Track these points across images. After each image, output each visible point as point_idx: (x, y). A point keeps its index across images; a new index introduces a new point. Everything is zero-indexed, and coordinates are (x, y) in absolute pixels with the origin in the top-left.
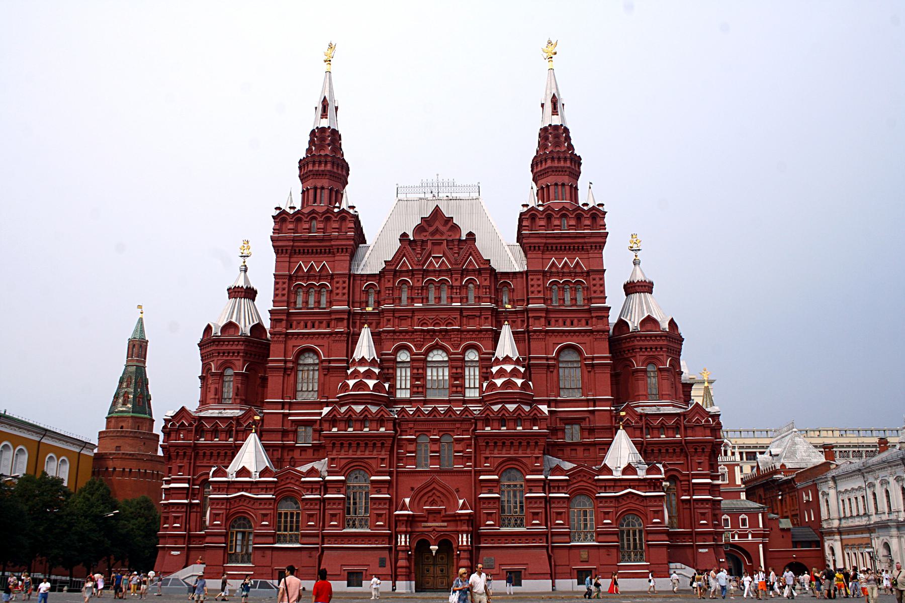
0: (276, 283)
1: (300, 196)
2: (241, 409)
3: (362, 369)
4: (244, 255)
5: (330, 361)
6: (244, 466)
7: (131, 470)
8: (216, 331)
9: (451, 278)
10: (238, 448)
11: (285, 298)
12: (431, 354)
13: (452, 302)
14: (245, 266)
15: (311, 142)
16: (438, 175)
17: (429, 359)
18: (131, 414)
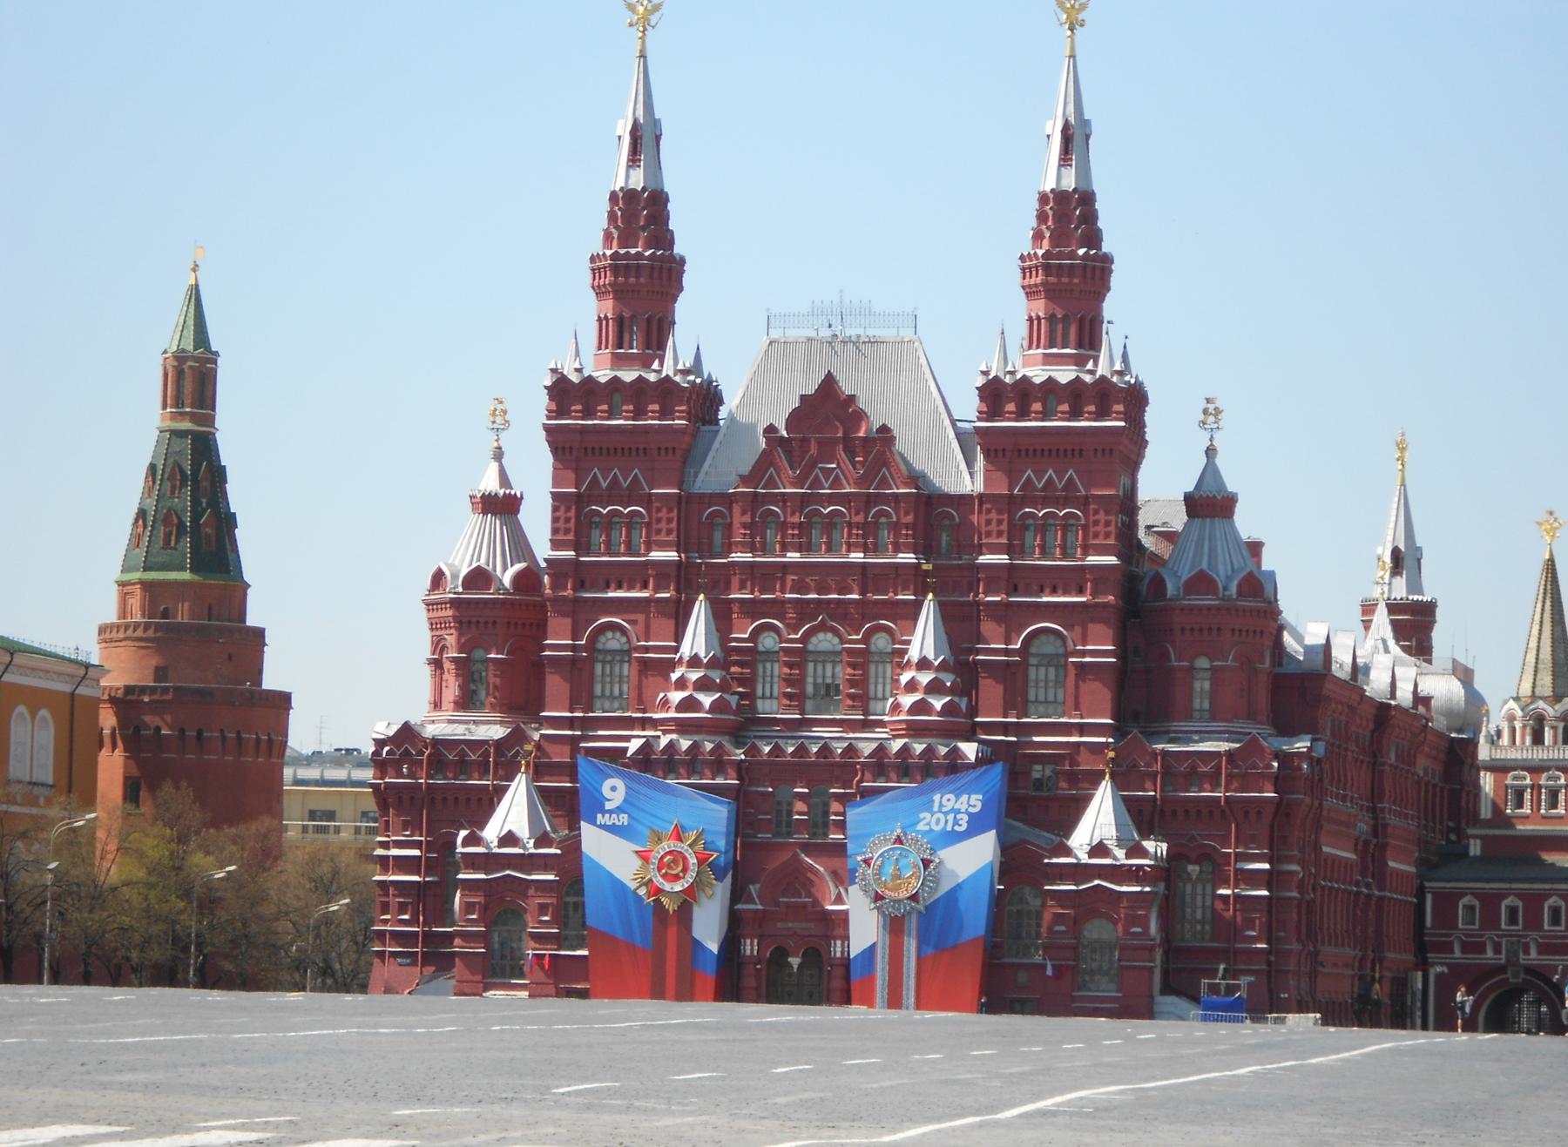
0: (555, 509)
1: (595, 325)
2: (501, 723)
3: (694, 676)
4: (496, 426)
5: (647, 649)
6: (510, 831)
7: (200, 733)
8: (454, 588)
9: (849, 509)
10: (500, 792)
11: (571, 537)
12: (814, 640)
13: (849, 551)
14: (500, 448)
15: (612, 217)
16: (841, 291)
17: (811, 647)
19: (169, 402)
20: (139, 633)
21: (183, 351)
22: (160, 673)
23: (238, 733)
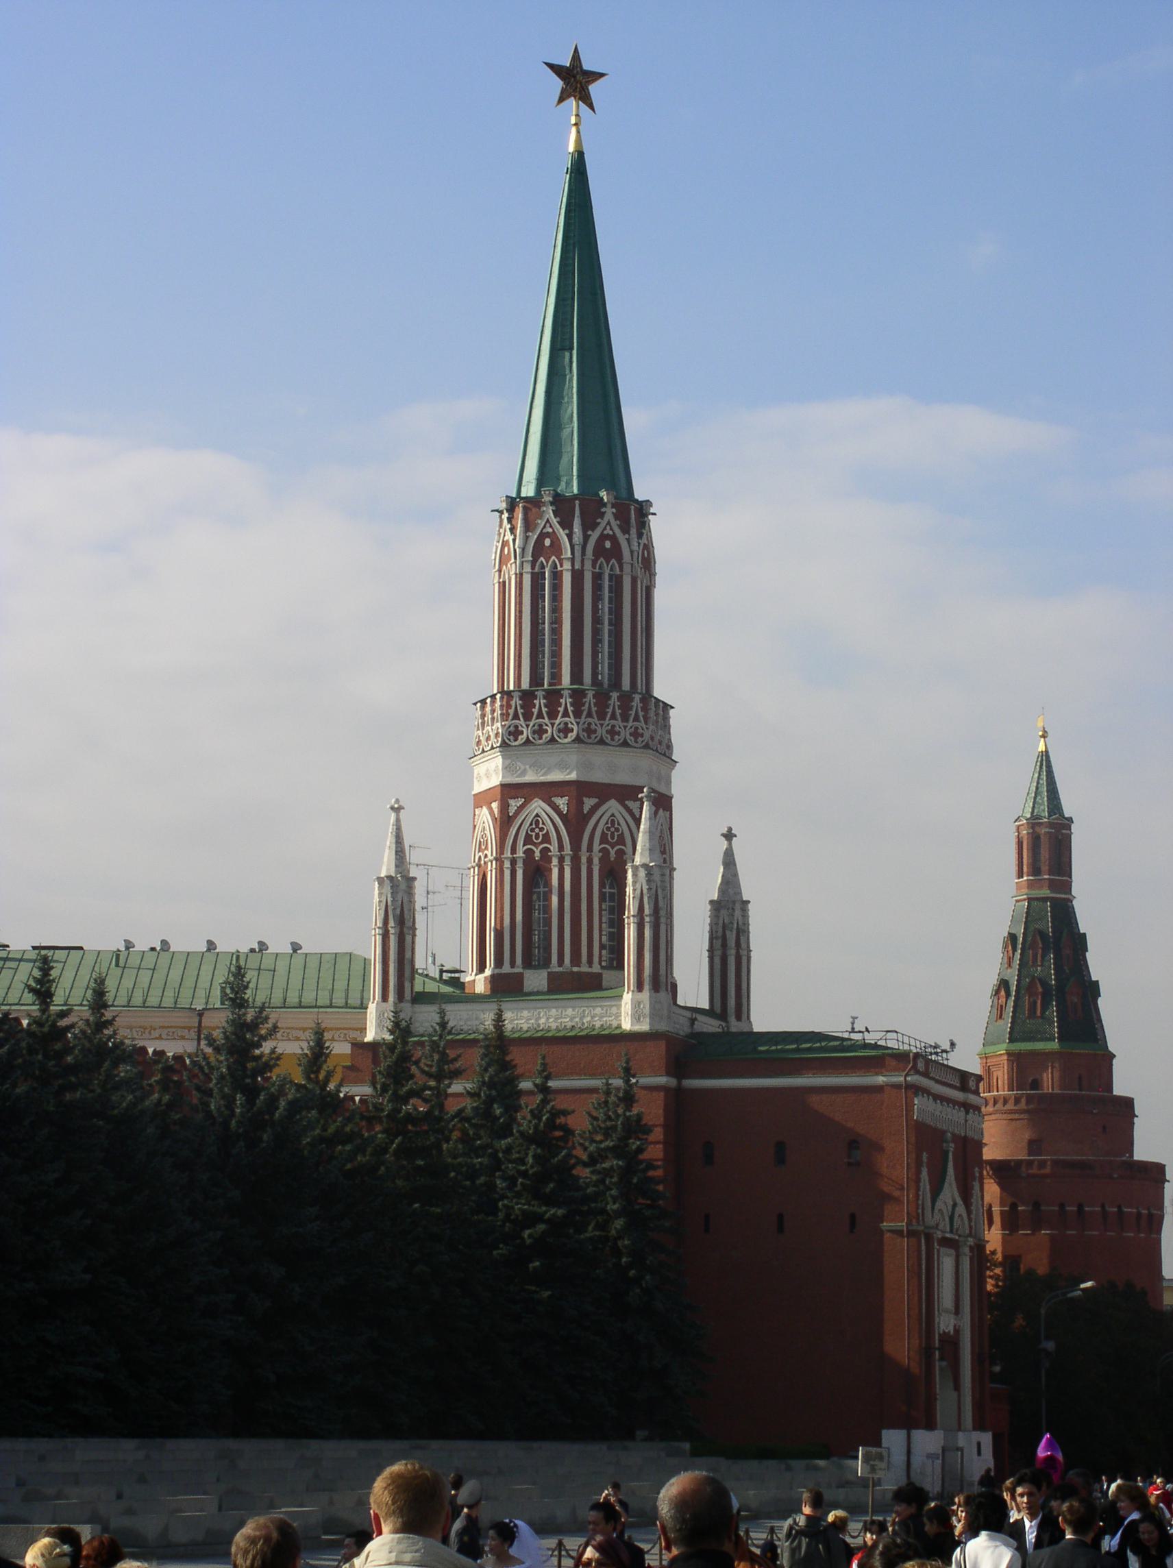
7: (1080, 1206)
18: (1054, 1045)
19: (1025, 869)
20: (1010, 1106)
21: (1039, 817)
22: (1034, 1146)
23: (1119, 1207)
